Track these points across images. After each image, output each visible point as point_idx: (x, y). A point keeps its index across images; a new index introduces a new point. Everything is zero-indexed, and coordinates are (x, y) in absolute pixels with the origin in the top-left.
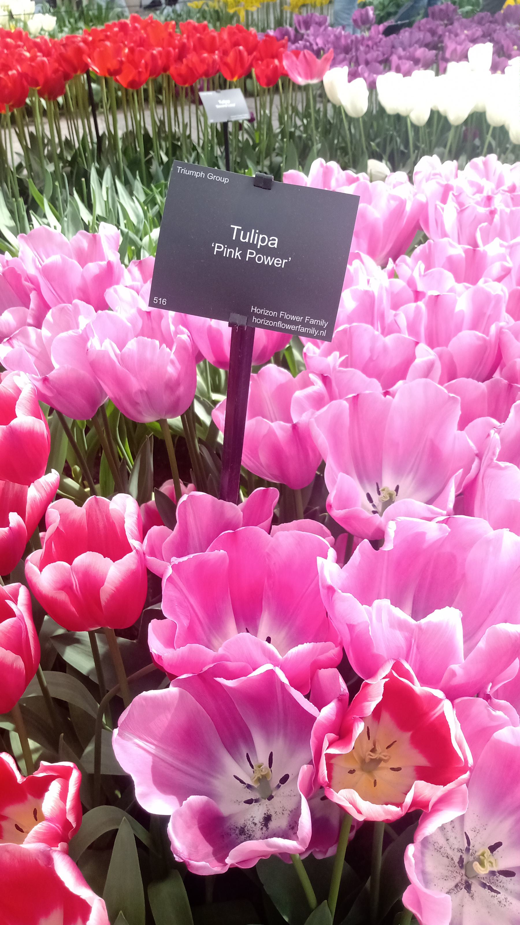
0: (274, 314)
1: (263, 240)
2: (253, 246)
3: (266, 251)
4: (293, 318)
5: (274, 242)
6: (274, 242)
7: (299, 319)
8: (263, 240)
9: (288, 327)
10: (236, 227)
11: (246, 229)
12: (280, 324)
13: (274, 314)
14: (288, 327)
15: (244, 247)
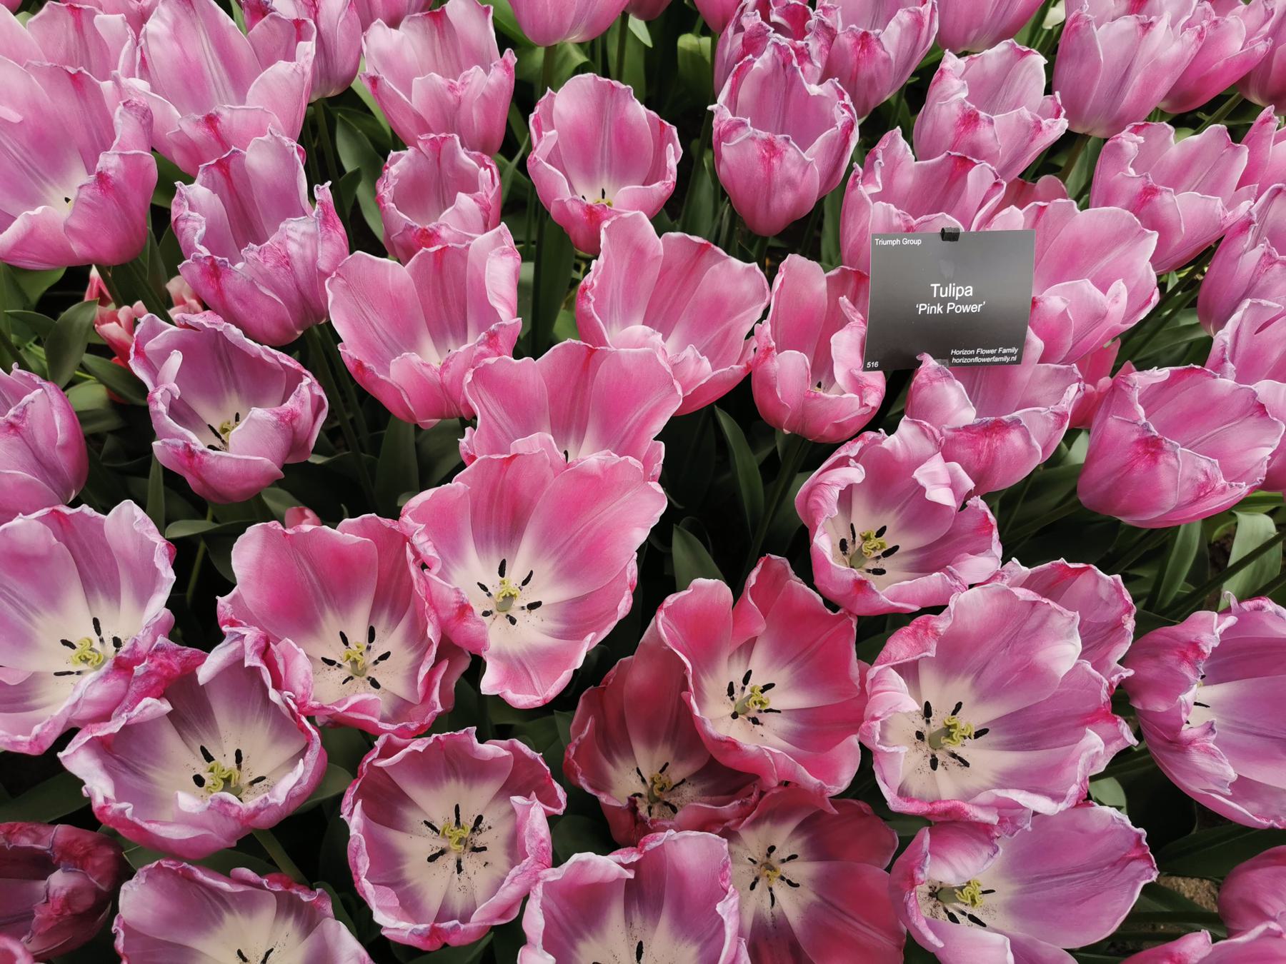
0: (972, 352)
1: (960, 291)
2: (952, 299)
3: (964, 301)
4: (988, 352)
5: (969, 291)
6: (969, 291)
7: (993, 351)
8: (960, 291)
9: (984, 360)
10: (935, 286)
11: (945, 285)
12: (977, 359)
13: (972, 352)
14: (984, 360)
15: (944, 302)
